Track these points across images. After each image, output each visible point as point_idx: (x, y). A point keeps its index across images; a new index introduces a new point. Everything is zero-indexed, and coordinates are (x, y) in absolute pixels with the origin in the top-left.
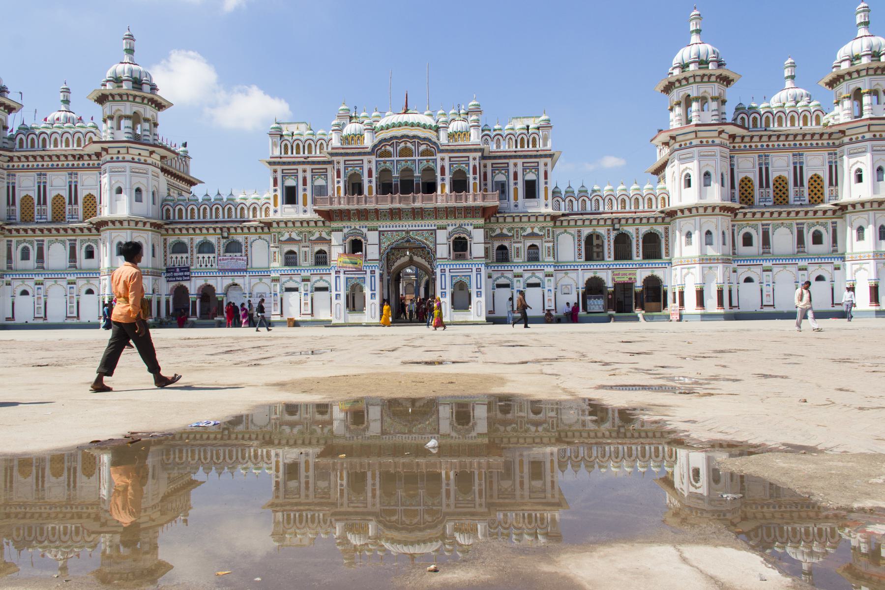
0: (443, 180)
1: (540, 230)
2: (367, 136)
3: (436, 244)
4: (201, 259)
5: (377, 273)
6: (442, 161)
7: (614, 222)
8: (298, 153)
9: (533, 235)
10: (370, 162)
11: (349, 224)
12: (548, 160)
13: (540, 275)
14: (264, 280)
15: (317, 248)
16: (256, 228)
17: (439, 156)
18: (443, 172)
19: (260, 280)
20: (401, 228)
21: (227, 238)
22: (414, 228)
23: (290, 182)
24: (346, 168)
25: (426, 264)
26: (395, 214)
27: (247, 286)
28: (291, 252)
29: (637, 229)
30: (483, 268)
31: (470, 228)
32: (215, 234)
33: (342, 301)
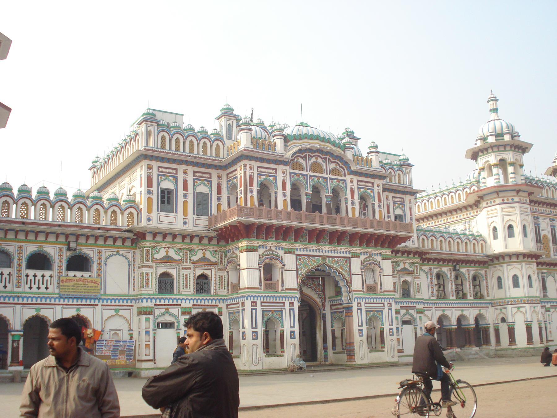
0: (353, 203)
1: (410, 266)
2: (279, 142)
3: (350, 274)
4: (31, 277)
5: (296, 305)
6: (351, 183)
7: (456, 262)
8: (177, 149)
9: (404, 270)
10: (283, 173)
11: (265, 244)
12: (412, 197)
13: (413, 312)
14: (121, 312)
15: (199, 272)
16: (115, 239)
17: (348, 178)
18: (352, 197)
19: (117, 311)
20: (318, 254)
21: (75, 249)
22: (330, 254)
23: (167, 185)
24: (259, 175)
25: (315, 297)
26: (316, 236)
27: (98, 319)
28: (166, 275)
29: (468, 271)
30: (393, 304)
31: (379, 258)
32: (56, 242)
33: (260, 341)
